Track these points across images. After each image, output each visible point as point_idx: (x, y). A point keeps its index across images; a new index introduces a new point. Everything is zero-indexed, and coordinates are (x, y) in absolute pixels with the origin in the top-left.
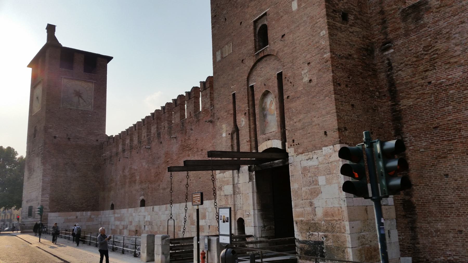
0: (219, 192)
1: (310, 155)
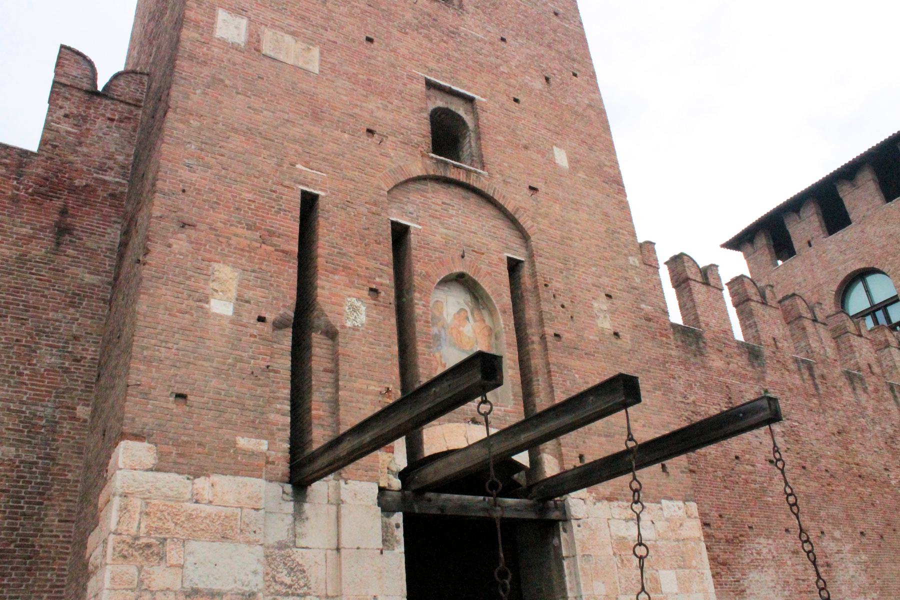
0: (130, 570)
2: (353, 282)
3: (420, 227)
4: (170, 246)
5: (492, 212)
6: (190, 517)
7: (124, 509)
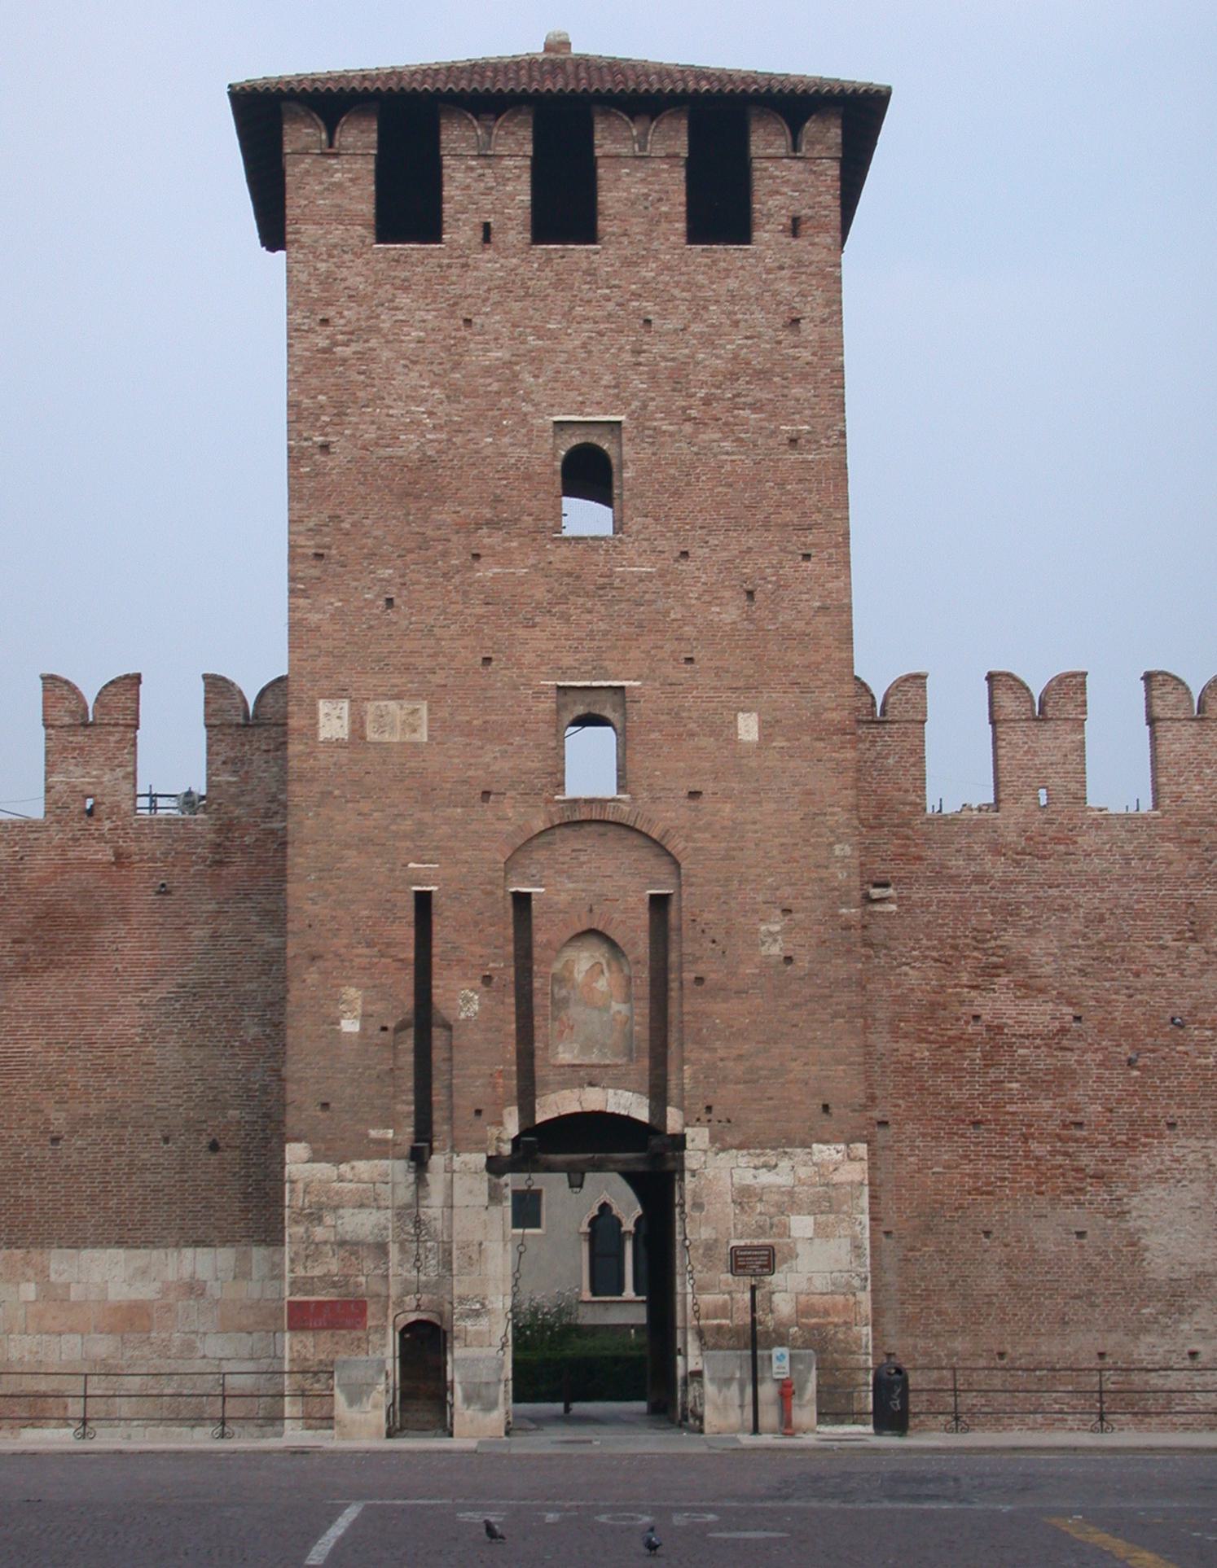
0: (300, 1230)
1: (770, 1156)
2: (465, 974)
3: (542, 890)
4: (304, 981)
5: (639, 841)
6: (337, 1193)
7: (292, 1191)
